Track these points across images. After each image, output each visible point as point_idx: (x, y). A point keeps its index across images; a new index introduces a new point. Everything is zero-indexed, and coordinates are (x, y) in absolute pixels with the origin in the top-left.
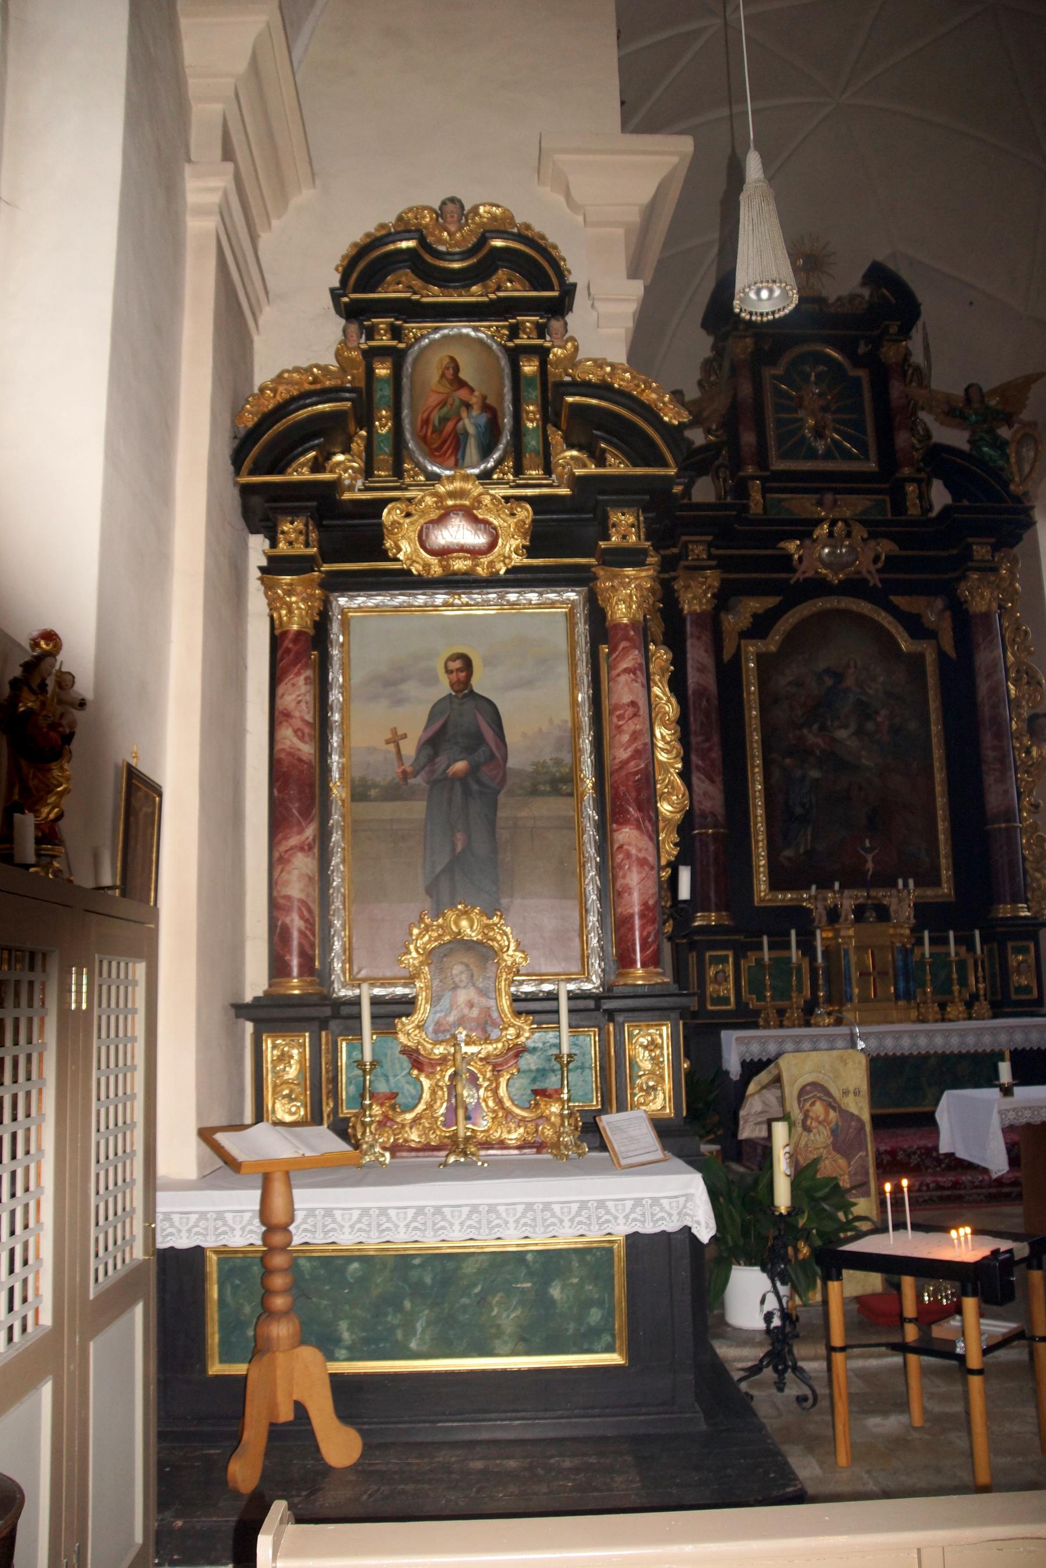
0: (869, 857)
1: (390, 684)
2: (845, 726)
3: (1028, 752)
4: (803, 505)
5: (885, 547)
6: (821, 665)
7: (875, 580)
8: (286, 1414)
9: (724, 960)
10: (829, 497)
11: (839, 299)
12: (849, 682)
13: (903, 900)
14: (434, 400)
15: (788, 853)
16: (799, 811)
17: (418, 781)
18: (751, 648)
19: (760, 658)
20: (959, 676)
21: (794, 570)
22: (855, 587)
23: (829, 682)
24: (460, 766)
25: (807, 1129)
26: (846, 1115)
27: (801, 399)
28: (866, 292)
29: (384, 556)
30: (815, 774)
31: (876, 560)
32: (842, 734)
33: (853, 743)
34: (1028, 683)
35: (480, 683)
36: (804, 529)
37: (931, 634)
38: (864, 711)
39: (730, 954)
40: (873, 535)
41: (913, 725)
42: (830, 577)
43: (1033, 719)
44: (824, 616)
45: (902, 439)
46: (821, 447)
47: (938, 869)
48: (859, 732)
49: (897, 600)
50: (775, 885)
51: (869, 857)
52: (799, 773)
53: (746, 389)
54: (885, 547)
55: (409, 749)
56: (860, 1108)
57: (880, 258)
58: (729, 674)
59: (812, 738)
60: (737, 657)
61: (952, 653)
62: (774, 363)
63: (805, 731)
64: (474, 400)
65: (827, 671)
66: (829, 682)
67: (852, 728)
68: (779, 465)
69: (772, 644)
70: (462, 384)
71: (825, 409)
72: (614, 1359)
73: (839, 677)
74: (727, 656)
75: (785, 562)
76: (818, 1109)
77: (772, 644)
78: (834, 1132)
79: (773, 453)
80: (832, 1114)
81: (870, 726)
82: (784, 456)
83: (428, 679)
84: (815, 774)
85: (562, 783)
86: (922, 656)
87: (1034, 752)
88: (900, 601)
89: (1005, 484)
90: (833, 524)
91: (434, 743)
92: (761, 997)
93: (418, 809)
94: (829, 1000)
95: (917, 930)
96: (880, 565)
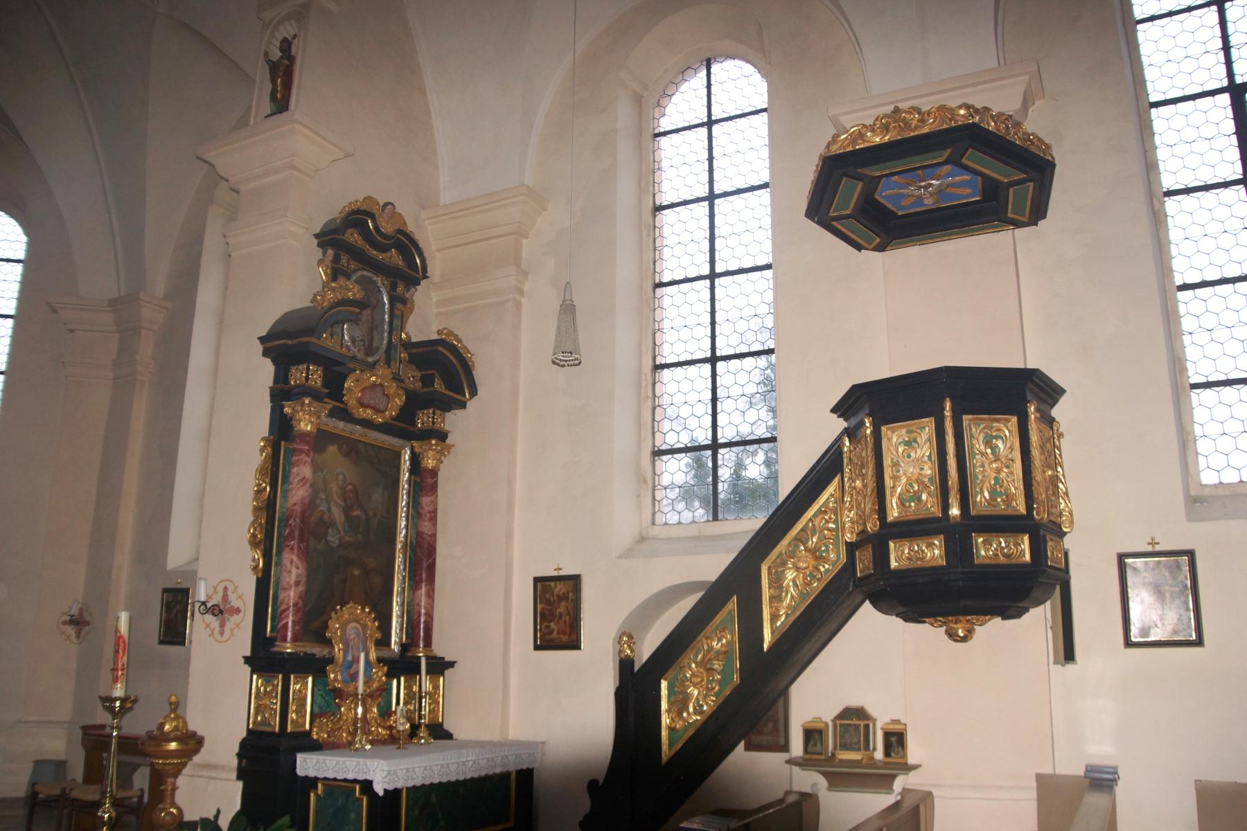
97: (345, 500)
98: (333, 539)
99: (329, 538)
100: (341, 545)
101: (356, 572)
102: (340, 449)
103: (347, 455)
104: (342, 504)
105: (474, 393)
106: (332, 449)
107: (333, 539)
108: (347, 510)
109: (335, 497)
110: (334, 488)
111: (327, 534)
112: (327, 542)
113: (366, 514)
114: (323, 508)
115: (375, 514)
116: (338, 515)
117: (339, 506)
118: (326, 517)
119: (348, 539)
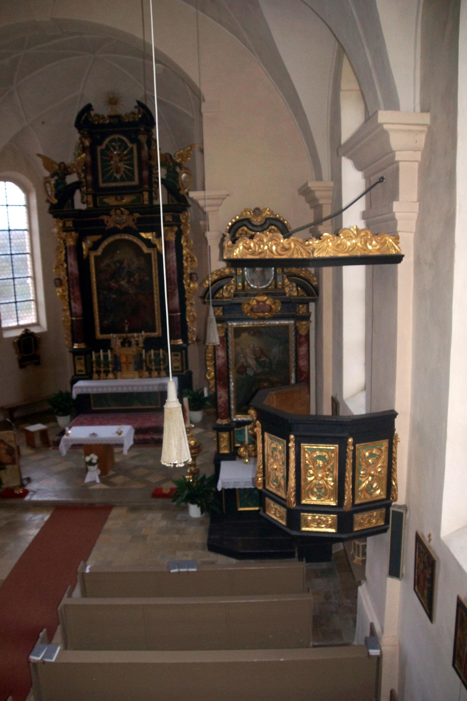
0: (127, 326)
2: (123, 280)
3: (189, 286)
4: (111, 201)
5: (137, 215)
6: (115, 259)
7: (134, 227)
10: (119, 197)
11: (126, 115)
12: (125, 264)
13: (140, 337)
15: (106, 322)
18: (93, 255)
19: (96, 258)
21: (105, 225)
22: (127, 230)
23: (118, 265)
26: (10, 447)
27: (111, 158)
28: (136, 111)
30: (114, 296)
31: (134, 220)
32: (123, 283)
34: (191, 261)
36: (107, 210)
38: (130, 274)
39: (83, 357)
40: (131, 213)
41: (147, 279)
42: (118, 226)
43: (191, 274)
44: (116, 241)
46: (118, 176)
48: (129, 282)
50: (102, 332)
51: (127, 326)
53: (89, 159)
54: (137, 215)
57: (138, 99)
58: (83, 264)
59: (113, 284)
60: (88, 257)
63: (110, 282)
65: (118, 261)
66: (118, 265)
67: (126, 280)
68: (102, 185)
69: (99, 251)
71: (120, 161)
73: (121, 262)
74: (85, 257)
75: (102, 223)
77: (99, 251)
79: (100, 180)
80: (6, 447)
81: (132, 279)
82: (104, 182)
84: (114, 296)
86: (150, 255)
87: (192, 285)
88: (143, 235)
89: (180, 190)
90: (116, 210)
94: (113, 371)
95: (143, 348)
96: (136, 222)
97: (255, 355)
98: (250, 372)
99: (248, 372)
100: (255, 374)
102: (249, 333)
104: (254, 357)
105: (318, 294)
106: (244, 335)
107: (250, 372)
110: (248, 351)
111: (246, 371)
112: (247, 374)
114: (243, 360)
116: (252, 362)
118: (245, 364)
119: (258, 371)
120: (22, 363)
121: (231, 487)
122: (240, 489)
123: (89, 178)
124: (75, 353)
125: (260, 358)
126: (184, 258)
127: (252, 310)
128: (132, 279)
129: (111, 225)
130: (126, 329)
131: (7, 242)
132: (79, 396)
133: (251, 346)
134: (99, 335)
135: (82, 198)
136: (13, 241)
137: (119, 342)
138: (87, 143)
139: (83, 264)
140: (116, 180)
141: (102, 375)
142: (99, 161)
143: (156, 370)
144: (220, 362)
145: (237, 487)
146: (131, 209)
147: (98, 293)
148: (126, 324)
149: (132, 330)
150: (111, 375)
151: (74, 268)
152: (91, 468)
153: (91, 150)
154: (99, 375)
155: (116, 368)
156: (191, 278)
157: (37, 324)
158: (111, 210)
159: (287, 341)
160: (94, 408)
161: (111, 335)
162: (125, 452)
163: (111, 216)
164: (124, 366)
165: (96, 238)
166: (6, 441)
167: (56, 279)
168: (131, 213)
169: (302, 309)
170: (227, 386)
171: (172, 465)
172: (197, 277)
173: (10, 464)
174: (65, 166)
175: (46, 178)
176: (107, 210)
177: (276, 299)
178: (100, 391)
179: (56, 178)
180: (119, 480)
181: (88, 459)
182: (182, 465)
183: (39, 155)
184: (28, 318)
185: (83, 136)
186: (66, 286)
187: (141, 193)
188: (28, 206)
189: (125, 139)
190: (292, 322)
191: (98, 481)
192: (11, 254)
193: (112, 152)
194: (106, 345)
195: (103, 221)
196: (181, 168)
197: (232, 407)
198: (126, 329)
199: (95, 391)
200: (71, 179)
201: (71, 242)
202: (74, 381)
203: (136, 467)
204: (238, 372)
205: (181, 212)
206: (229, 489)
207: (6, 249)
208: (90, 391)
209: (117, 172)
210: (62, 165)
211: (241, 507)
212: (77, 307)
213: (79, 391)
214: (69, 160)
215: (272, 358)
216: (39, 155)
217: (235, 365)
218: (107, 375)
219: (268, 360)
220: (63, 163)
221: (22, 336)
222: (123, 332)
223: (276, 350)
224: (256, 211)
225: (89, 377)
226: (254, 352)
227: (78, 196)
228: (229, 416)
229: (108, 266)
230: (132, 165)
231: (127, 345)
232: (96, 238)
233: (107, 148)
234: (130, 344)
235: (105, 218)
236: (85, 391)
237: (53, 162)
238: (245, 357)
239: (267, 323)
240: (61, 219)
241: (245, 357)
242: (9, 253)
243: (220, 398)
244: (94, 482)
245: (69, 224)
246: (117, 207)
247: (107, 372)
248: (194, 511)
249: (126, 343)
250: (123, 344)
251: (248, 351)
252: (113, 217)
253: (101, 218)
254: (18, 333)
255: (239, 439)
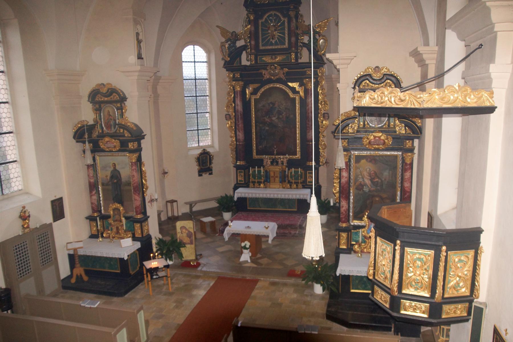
1: (104, 168)
2: (275, 117)
3: (322, 122)
4: (267, 59)
5: (286, 70)
6: (269, 102)
7: (284, 78)
8: (79, 275)
9: (242, 172)
10: (274, 57)
12: (276, 105)
13: (284, 159)
14: (106, 119)
15: (261, 147)
16: (263, 137)
17: (110, 183)
18: (253, 97)
19: (255, 99)
20: (304, 103)
22: (279, 81)
23: (271, 106)
24: (115, 181)
25: (182, 233)
26: (189, 232)
27: (269, 28)
29: (100, 147)
30: (267, 128)
31: (284, 74)
32: (274, 118)
33: (276, 121)
35: (118, 168)
37: (298, 92)
38: (280, 113)
40: (282, 69)
41: (292, 116)
43: (324, 114)
45: (293, 39)
47: (296, 151)
48: (278, 118)
49: (290, 84)
50: (257, 154)
52: (263, 128)
53: (253, 29)
54: (286, 70)
55: (108, 178)
56: (192, 231)
58: (246, 104)
59: (267, 119)
60: (250, 99)
61: (303, 98)
62: (262, 18)
64: (112, 118)
65: (271, 103)
66: (271, 106)
68: (261, 48)
70: (110, 115)
71: (275, 30)
72: (119, 272)
73: (274, 104)
76: (184, 230)
78: (187, 234)
80: (187, 232)
81: (281, 116)
82: (263, 46)
83: (110, 167)
84: (267, 128)
85: (129, 184)
86: (295, 99)
87: (324, 122)
88: (290, 84)
90: (271, 66)
91: (112, 177)
92: (255, 179)
93: (110, 187)
94: (264, 182)
95: (286, 166)
98: (366, 189)
99: (364, 189)
100: (370, 191)
101: (377, 199)
102: (367, 160)
103: (370, 161)
105: (421, 133)
106: (363, 161)
107: (366, 189)
108: (372, 180)
109: (366, 176)
110: (365, 174)
112: (363, 191)
113: (381, 180)
114: (361, 180)
115: (385, 180)
116: (368, 182)
117: (368, 179)
119: (372, 189)
120: (201, 173)
121: (347, 274)
122: (353, 276)
123: (253, 43)
124: (238, 167)
125: (374, 179)
126: (320, 102)
127: (370, 142)
128: (281, 116)
129: (267, 76)
130: (275, 152)
131: (194, 87)
132: (238, 198)
133: (368, 169)
134: (255, 156)
135: (247, 57)
136: (198, 87)
137: (269, 162)
138: (252, 18)
139: (246, 104)
140: (272, 44)
141: (256, 184)
142: (260, 30)
143: (295, 183)
144: (344, 180)
145: (351, 274)
146: (282, 65)
147: (256, 126)
148: (275, 149)
149: (278, 154)
150: (262, 185)
151: (240, 108)
152: (245, 251)
153: (255, 23)
154: (254, 185)
155: (267, 180)
156: (324, 117)
157: (212, 146)
158: (268, 66)
159: (395, 168)
160: (248, 208)
161: (264, 156)
162: (270, 242)
163: (267, 70)
164: (272, 179)
165: (256, 86)
166: (187, 227)
167: (226, 115)
168: (282, 69)
169: (408, 144)
170: (348, 198)
171: (310, 258)
172: (328, 116)
173: (189, 244)
174: (236, 34)
175: (222, 43)
176: (265, 66)
177: (389, 135)
178: (254, 196)
179: (229, 43)
180: (264, 261)
181: (243, 244)
182: (318, 259)
183: (218, 26)
184: (206, 141)
185: (249, 12)
186: (234, 120)
187: (290, 53)
188: (208, 62)
189: (279, 14)
190: (400, 153)
191: (249, 261)
192: (196, 96)
193: (270, 24)
194: (260, 163)
195: (261, 73)
196: (319, 36)
197: (351, 214)
198: (275, 152)
199: (250, 196)
200: (240, 43)
201: (238, 89)
202: (236, 188)
203: (277, 253)
204: (357, 189)
205: (318, 68)
206: (345, 275)
207: (193, 92)
208: (247, 196)
209: (273, 39)
210: (234, 33)
211: (353, 289)
212: (241, 135)
213: (240, 195)
214: (240, 30)
215: (383, 179)
216: (218, 26)
217: (355, 184)
218: (260, 185)
219: (380, 181)
220: (235, 32)
221: (201, 154)
222: (273, 154)
223: (386, 174)
224: (377, 69)
225: (246, 185)
226: (370, 175)
227: (244, 55)
228: (348, 221)
229: (264, 106)
230: (284, 34)
231: (275, 164)
232: (256, 86)
233: (266, 20)
234: (277, 163)
235: (264, 72)
236: (243, 196)
237: (227, 31)
238: (363, 178)
239: (381, 153)
240: (232, 72)
241: (363, 178)
242: (195, 95)
243: (343, 207)
244: (246, 262)
245: (238, 75)
246: (272, 64)
247: (259, 183)
248: (318, 289)
249: (274, 162)
250: (272, 163)
251: (365, 174)
252: (269, 71)
253: (260, 71)
254: (200, 151)
255: (355, 239)
